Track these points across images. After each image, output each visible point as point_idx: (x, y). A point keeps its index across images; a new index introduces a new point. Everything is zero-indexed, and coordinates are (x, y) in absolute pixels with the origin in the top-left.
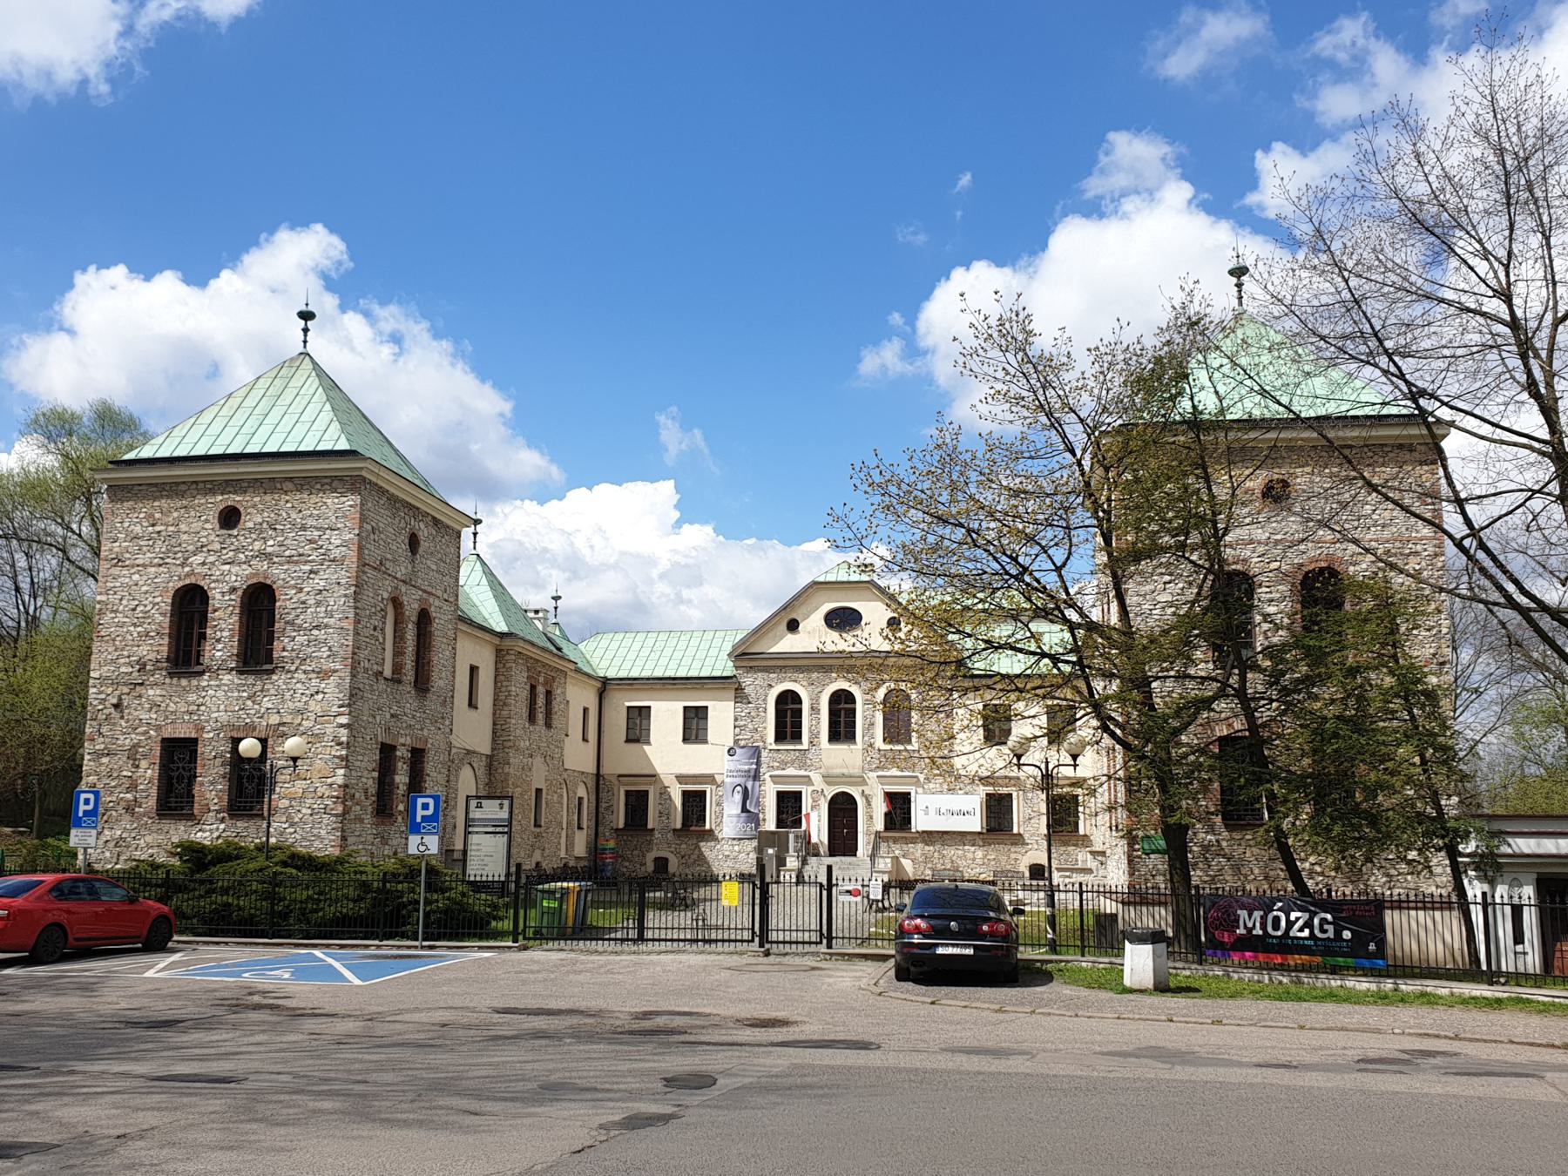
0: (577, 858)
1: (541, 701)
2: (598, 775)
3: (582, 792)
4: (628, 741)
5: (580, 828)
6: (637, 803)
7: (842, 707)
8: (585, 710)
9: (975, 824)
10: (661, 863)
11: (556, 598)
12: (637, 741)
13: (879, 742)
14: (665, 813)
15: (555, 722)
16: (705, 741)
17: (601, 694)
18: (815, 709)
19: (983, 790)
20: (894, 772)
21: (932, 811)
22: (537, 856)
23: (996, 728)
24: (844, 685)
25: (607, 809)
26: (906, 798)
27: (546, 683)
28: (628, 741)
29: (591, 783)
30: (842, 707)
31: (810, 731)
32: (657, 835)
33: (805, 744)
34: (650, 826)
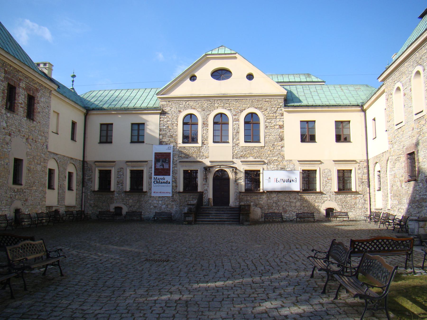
0: (67, 207)
1: (21, 99)
2: (84, 162)
3: (71, 168)
4: (101, 142)
5: (70, 189)
6: (105, 176)
7: (221, 121)
8: (74, 124)
9: (296, 186)
10: (119, 209)
11: (74, 76)
12: (107, 142)
13: (242, 143)
14: (120, 183)
15: (38, 117)
16: (143, 142)
17: (86, 116)
18: (205, 124)
19: (300, 168)
20: (251, 159)
21: (272, 180)
22: (18, 204)
23: (308, 135)
24: (220, 110)
25: (89, 180)
26: (257, 173)
27: (28, 89)
28: (101, 142)
29: (79, 166)
30: (221, 121)
31: (202, 137)
32: (116, 195)
33: (199, 144)
34: (112, 189)
